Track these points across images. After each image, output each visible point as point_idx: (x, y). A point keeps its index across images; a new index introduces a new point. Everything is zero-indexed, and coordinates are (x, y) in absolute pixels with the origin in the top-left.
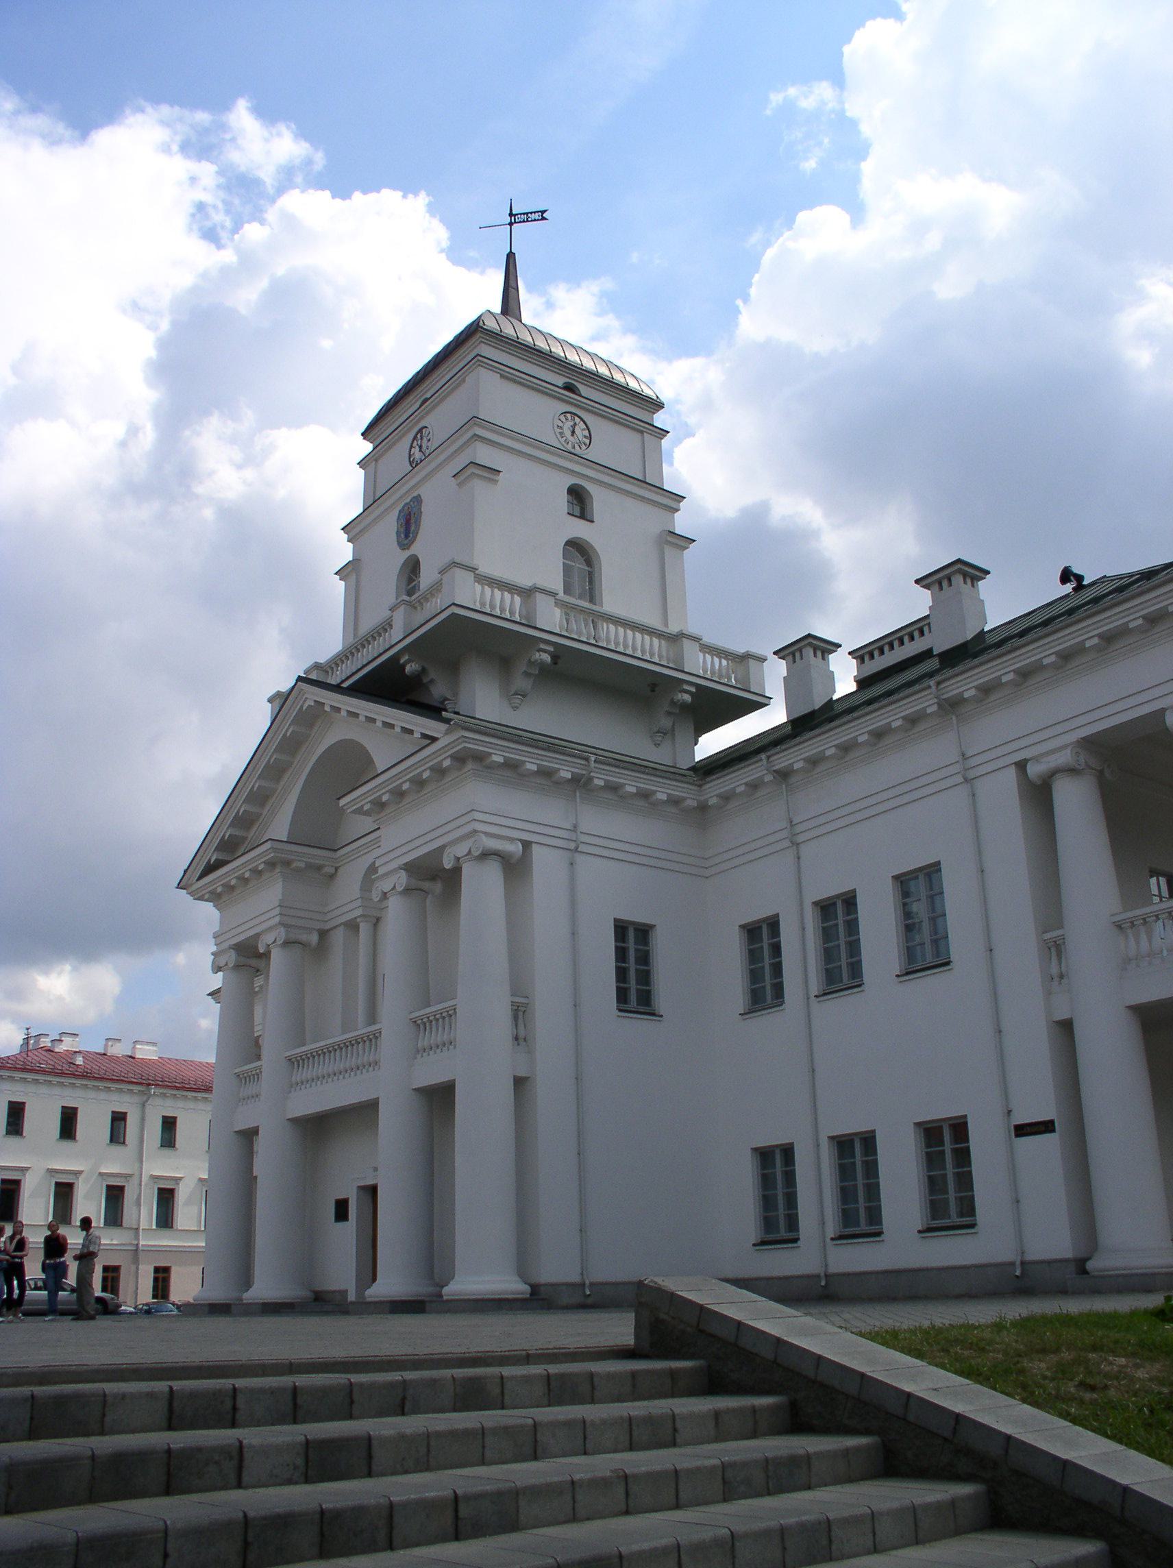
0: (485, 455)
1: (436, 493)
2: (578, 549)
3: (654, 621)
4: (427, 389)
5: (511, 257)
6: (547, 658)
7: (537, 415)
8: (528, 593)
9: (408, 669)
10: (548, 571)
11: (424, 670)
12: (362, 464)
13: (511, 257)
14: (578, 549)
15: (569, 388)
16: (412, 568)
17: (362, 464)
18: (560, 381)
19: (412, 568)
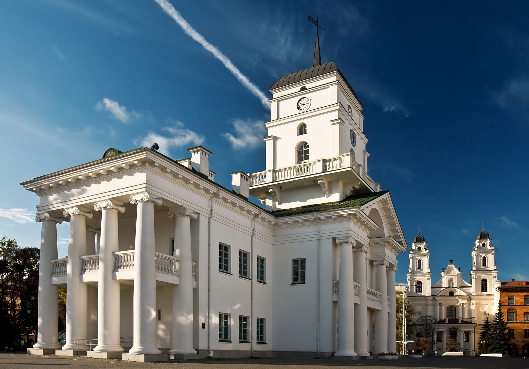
19: (304, 145)
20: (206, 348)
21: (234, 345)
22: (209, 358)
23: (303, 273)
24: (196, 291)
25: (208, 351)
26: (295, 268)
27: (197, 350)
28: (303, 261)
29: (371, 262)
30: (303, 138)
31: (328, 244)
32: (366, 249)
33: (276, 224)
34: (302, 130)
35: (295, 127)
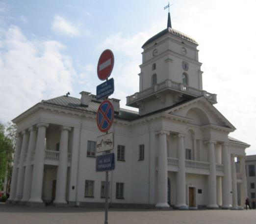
0: (170, 57)
1: (159, 63)
2: (185, 74)
3: (198, 88)
4: (158, 41)
5: (169, 14)
6: (181, 96)
7: (176, 47)
8: (179, 84)
9: (158, 97)
10: (179, 79)
11: (160, 97)
12: (142, 53)
13: (169, 14)
14: (185, 74)
15: (183, 43)
16: (155, 76)
17: (142, 53)
18: (181, 41)
19: (155, 76)
20: (74, 201)
21: (97, 198)
22: (76, 206)
23: (143, 153)
24: (69, 169)
25: (75, 202)
26: (141, 150)
27: (68, 202)
28: (143, 146)
29: (204, 141)
30: (155, 71)
31: (153, 135)
32: (183, 136)
33: (131, 125)
34: (154, 67)
35: (152, 64)
